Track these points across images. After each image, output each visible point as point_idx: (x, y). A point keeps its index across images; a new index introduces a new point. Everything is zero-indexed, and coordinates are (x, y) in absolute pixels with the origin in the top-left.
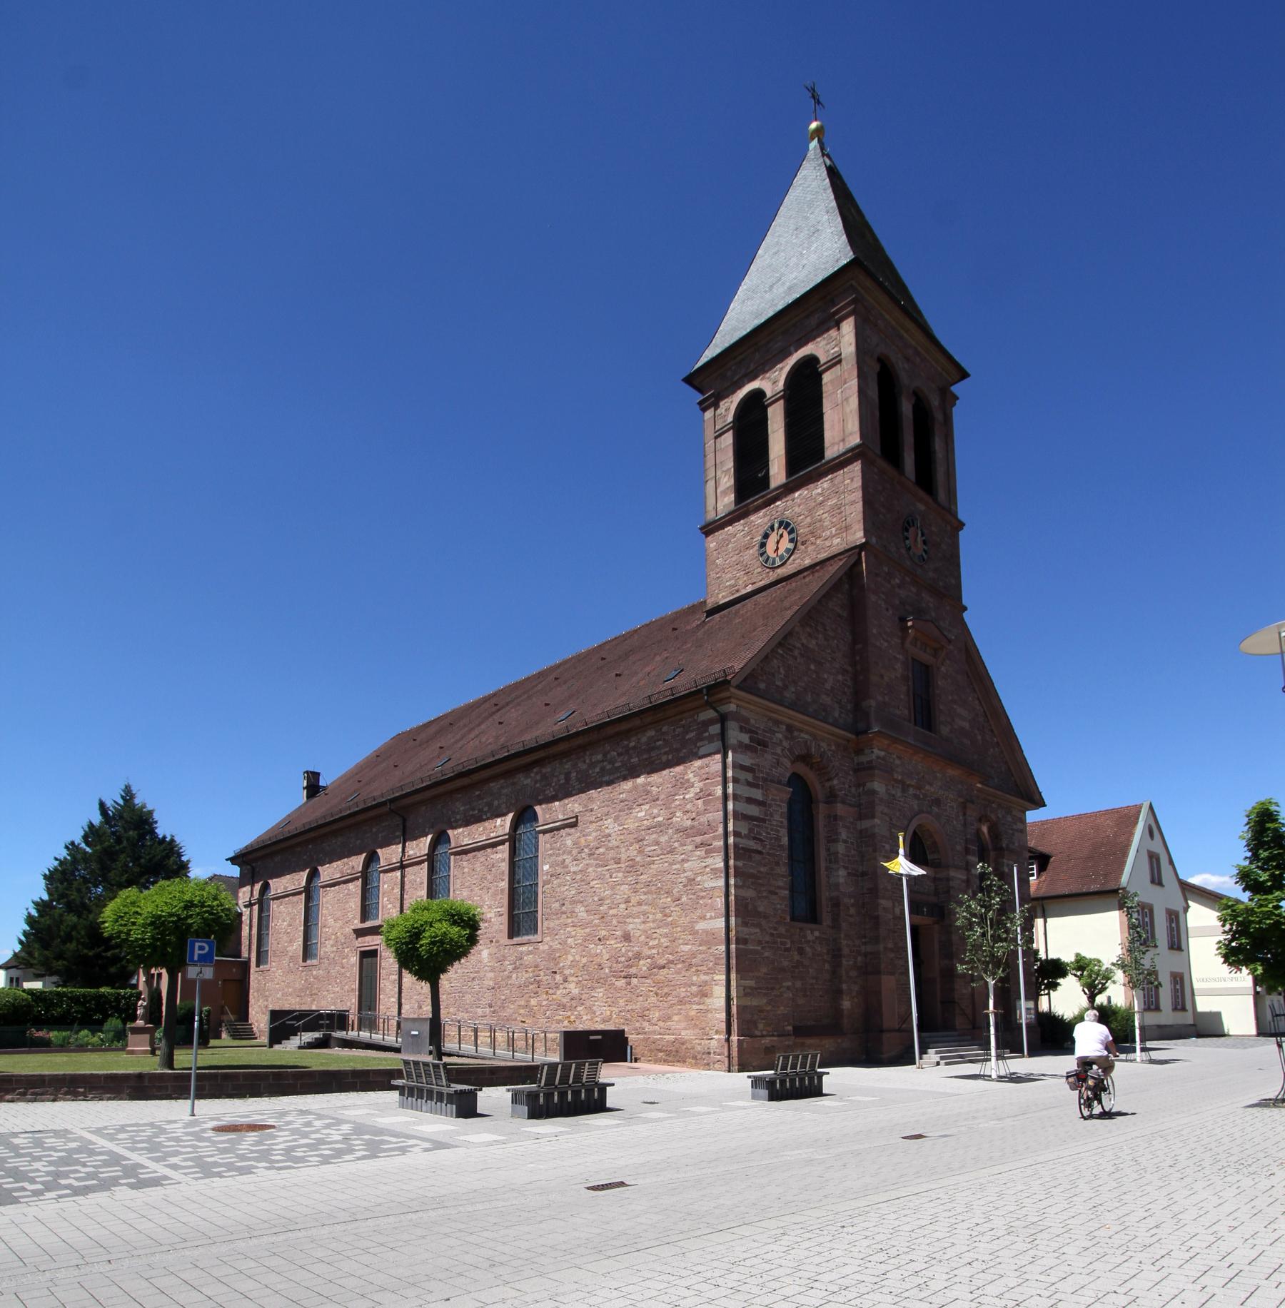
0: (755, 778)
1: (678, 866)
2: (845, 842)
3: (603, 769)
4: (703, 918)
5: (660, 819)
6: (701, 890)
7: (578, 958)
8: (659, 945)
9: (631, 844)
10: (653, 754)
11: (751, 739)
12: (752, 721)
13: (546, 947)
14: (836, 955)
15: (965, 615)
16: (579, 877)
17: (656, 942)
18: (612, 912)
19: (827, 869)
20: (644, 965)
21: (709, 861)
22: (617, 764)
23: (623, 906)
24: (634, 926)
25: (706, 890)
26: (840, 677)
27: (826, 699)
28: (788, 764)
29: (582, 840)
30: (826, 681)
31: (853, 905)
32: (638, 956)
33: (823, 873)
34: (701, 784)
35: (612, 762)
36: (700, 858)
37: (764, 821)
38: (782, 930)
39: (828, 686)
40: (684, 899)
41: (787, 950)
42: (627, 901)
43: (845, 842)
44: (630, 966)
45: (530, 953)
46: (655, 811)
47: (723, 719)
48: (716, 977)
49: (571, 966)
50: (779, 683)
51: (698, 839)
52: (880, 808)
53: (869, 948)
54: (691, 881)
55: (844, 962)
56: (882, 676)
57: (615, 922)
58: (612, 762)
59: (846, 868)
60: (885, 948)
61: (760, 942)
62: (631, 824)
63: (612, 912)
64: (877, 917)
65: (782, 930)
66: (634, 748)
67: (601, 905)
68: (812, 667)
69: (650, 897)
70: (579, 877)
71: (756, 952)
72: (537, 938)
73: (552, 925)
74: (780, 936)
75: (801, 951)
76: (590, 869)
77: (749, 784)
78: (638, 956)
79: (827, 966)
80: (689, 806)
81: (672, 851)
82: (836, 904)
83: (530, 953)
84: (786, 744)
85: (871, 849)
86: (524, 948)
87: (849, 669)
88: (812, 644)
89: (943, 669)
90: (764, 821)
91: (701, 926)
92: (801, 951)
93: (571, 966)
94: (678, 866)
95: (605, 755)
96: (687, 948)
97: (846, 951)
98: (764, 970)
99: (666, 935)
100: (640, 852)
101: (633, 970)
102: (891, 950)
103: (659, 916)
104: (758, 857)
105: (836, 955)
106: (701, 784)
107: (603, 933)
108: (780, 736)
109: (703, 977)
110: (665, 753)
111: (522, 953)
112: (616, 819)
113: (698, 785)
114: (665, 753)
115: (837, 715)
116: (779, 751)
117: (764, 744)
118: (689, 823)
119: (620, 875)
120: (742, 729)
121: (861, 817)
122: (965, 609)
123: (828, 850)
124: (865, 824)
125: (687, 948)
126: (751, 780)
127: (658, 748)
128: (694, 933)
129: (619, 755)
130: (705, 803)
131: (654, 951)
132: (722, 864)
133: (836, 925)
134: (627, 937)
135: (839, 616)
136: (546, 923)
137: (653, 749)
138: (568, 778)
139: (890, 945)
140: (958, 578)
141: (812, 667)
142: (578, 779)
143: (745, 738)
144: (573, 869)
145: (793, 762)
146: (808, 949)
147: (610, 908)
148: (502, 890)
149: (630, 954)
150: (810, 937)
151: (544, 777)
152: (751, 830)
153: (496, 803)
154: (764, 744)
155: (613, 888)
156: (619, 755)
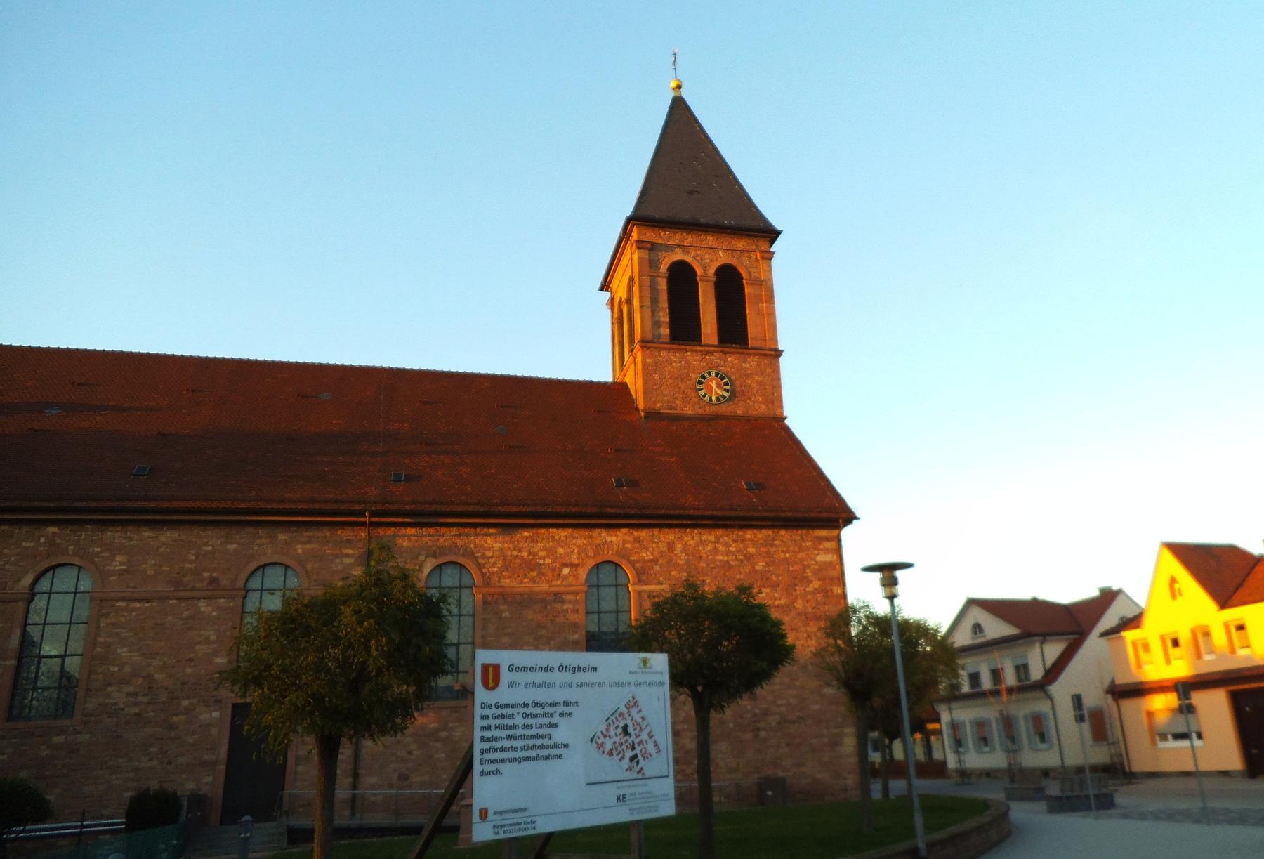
3: (716, 550)
10: (772, 550)
20: (773, 720)
32: (766, 713)
35: (726, 545)
66: (751, 539)
78: (766, 713)
80: (809, 597)
95: (718, 538)
96: (817, 707)
109: (835, 731)
113: (816, 584)
125: (817, 707)
127: (776, 546)
129: (735, 541)
137: (772, 545)
142: (683, 551)
149: (757, 711)
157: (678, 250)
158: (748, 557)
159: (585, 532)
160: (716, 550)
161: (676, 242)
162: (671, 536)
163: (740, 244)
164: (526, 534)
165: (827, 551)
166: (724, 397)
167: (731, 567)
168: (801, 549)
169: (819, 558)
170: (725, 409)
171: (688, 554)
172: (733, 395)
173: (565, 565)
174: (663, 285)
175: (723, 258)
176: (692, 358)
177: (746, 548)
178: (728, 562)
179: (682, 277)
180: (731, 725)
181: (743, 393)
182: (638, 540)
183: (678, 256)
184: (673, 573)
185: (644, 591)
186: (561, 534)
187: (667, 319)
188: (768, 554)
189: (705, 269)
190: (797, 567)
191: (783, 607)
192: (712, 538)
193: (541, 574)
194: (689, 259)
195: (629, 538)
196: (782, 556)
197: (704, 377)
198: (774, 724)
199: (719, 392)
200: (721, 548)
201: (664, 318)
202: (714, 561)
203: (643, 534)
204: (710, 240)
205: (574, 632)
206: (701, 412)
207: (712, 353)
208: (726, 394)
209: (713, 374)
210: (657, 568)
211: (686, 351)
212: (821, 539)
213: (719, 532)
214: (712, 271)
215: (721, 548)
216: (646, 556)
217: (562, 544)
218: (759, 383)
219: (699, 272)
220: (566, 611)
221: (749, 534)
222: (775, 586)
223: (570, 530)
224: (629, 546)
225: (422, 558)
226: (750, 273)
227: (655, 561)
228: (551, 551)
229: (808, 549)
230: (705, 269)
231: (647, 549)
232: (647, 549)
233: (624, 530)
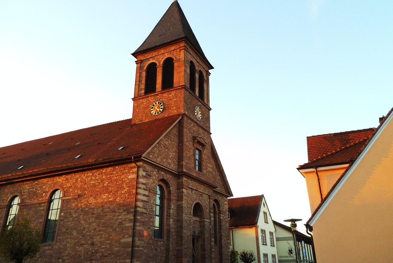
0: (147, 187)
1: (116, 217)
2: (173, 209)
3: (91, 179)
4: (124, 237)
5: (112, 199)
6: (124, 227)
7: (70, 252)
8: (106, 248)
9: (99, 208)
11: (146, 174)
12: (147, 168)
13: (57, 247)
14: (168, 250)
15: (211, 135)
16: (76, 219)
17: (104, 247)
18: (88, 234)
19: (167, 219)
21: (128, 216)
22: (97, 178)
23: (92, 231)
24: (97, 239)
25: (126, 227)
26: (174, 154)
27: (170, 161)
28: (157, 183)
29: (80, 205)
30: (170, 155)
31: (174, 232)
32: (96, 252)
33: (165, 220)
34: (128, 188)
35: (96, 177)
36: (125, 215)
37: (148, 202)
38: (151, 242)
39: (171, 157)
40: (117, 229)
41: (152, 249)
42: (95, 230)
43: (173, 209)
44: (93, 256)
45: (49, 249)
46: (110, 196)
47: (139, 167)
48: (127, 261)
49: (67, 256)
50: (156, 156)
51: (125, 208)
52: (184, 198)
53: (179, 248)
54: (121, 223)
55: (170, 253)
56: (187, 154)
57: (88, 238)
58: (96, 177)
59: (172, 218)
60: (184, 248)
61: (143, 247)
62: (100, 200)
63: (88, 234)
64: (182, 236)
65: (151, 242)
66: (105, 173)
67: (84, 230)
68: (166, 150)
69: (104, 229)
70: (76, 219)
71: (141, 250)
72: (54, 243)
73: (61, 238)
74: (150, 244)
75: (156, 249)
76: (81, 216)
77: (144, 189)
78: (96, 252)
79: (164, 255)
81: (114, 212)
82: (169, 231)
83: (49, 249)
84: (156, 175)
85: (181, 212)
86: (47, 248)
87: (177, 151)
88: (167, 143)
89: (204, 152)
90: (148, 202)
91: (123, 240)
92: (156, 249)
93: (67, 256)
94: (116, 217)
95: (93, 174)
96: (117, 249)
97: (171, 249)
98: (144, 257)
99: (109, 244)
100: (102, 211)
101: (94, 258)
102: (186, 249)
103: (107, 236)
104: (145, 215)
105: (168, 250)
106: (128, 188)
107: (83, 242)
108: (155, 173)
109: (122, 261)
110: (116, 176)
111: (46, 249)
112: (95, 198)
113: (127, 189)
114: (116, 176)
115: (173, 166)
116: (154, 178)
117: (150, 175)
118: (122, 202)
119: (93, 219)
120: (144, 171)
121: (178, 201)
122: (211, 134)
123: (167, 212)
124: (180, 203)
125: (117, 249)
126: (145, 188)
128: (120, 243)
129: (99, 174)
130: (128, 195)
131: (103, 250)
132: (133, 218)
133: (168, 240)
134: (93, 244)
135: (175, 134)
136: (58, 238)
137: (112, 174)
138: (76, 181)
139: (186, 247)
140: (209, 124)
141: (166, 150)
142: (80, 182)
143: (144, 174)
144: (74, 216)
145: (158, 182)
146: (159, 249)
147: (87, 232)
148: (41, 223)
149: (93, 251)
150: (160, 244)
151: (67, 179)
152: (144, 206)
153: (44, 187)
154: (150, 175)
155: (89, 224)
156: (99, 174)
157: (151, 59)
158: (102, 180)
159: (52, 179)
160: (91, 179)
161: (150, 56)
162: (77, 176)
163: (173, 48)
164: (36, 182)
165: (133, 173)
166: (160, 111)
167: (96, 186)
168: (123, 174)
169: (129, 177)
170: (159, 117)
171: (81, 183)
172: (164, 109)
173: (44, 192)
174: (144, 74)
175: (167, 56)
176: (151, 99)
177: (102, 176)
178: (95, 184)
179: (152, 69)
180: (83, 258)
181: (168, 107)
182: (67, 179)
183: (152, 61)
184: (76, 191)
185: (64, 200)
186: (45, 180)
187: (144, 87)
188: (110, 178)
189: (159, 62)
190: (120, 182)
191: (111, 201)
192: (91, 174)
193: (37, 197)
194: (154, 61)
195: (64, 179)
196: (115, 178)
197: (154, 105)
198: (98, 257)
199: (158, 110)
200: (94, 178)
201: (143, 86)
202: (90, 184)
203: (69, 177)
204: (162, 51)
205: (41, 218)
206: (152, 119)
207: (158, 95)
208: (161, 110)
209: (157, 103)
210: (71, 190)
211: (148, 97)
212: (131, 168)
213: (94, 171)
214: (162, 63)
215: (94, 178)
216: (69, 185)
217: (45, 184)
218: (175, 101)
219: (158, 64)
220: (41, 210)
221: (104, 171)
222: (109, 193)
223: (48, 179)
224: (64, 182)
225: (9, 195)
226: (176, 58)
227: (70, 187)
228: (41, 187)
229: (126, 173)
230: (159, 62)
231: (69, 182)
232: (69, 182)
233: (63, 176)
